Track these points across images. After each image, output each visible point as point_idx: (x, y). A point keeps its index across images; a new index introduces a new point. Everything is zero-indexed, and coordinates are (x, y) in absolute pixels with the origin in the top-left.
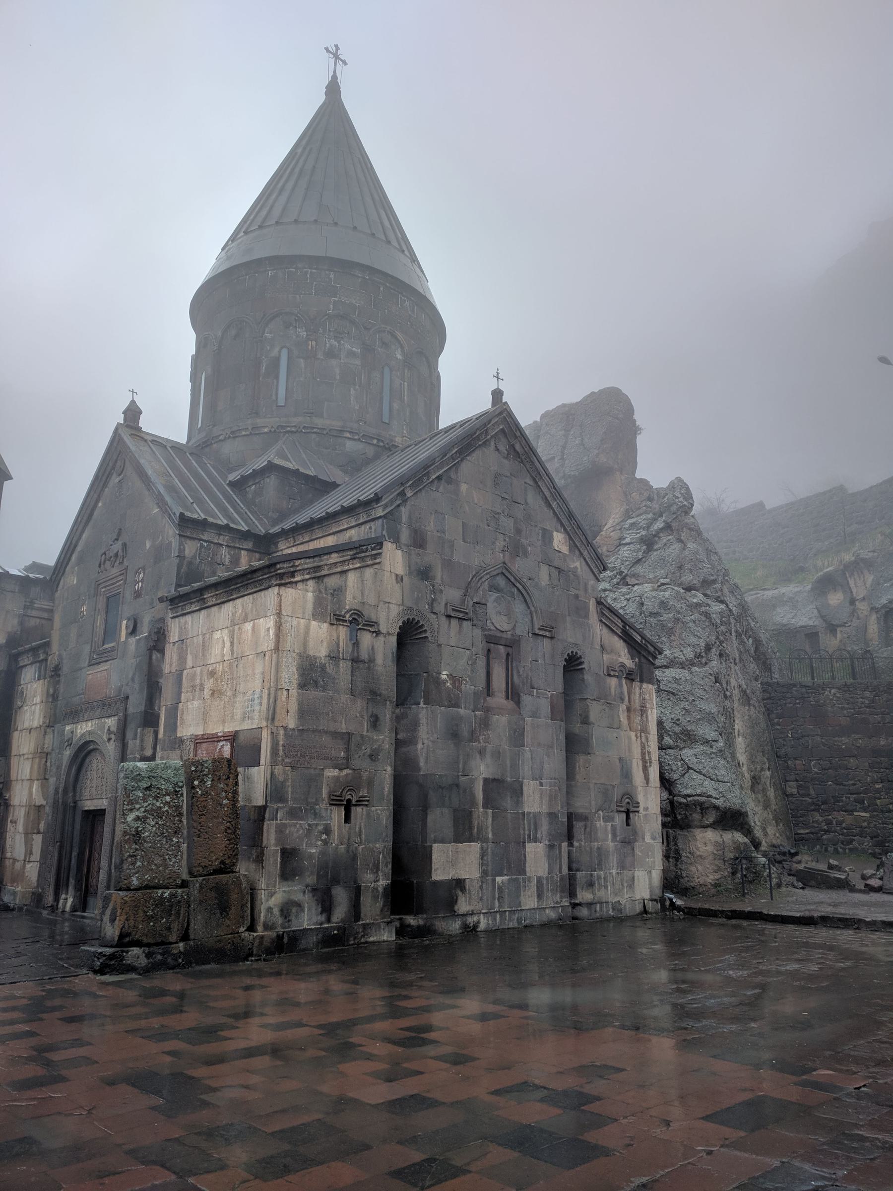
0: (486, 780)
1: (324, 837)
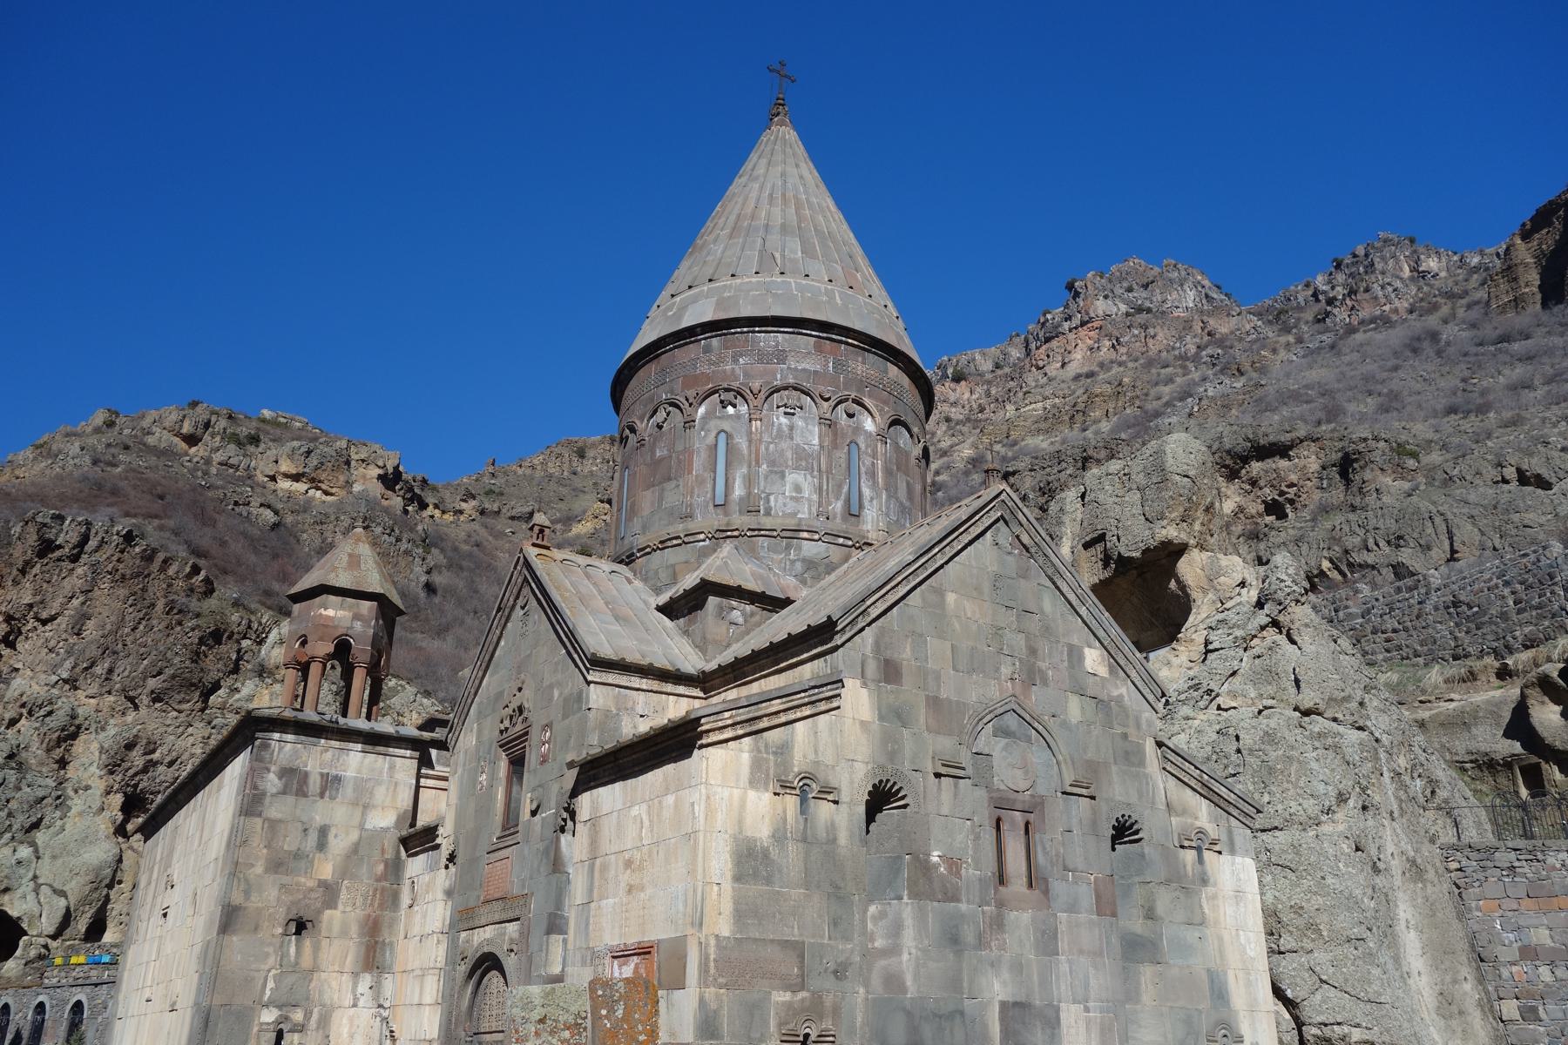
0: (1003, 1005)
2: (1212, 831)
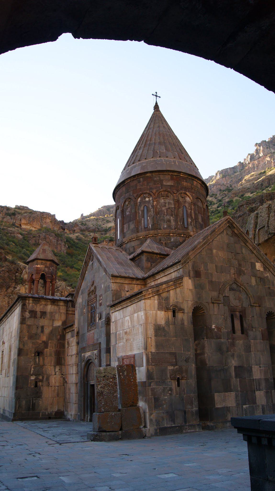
0: (235, 367)
1: (170, 392)
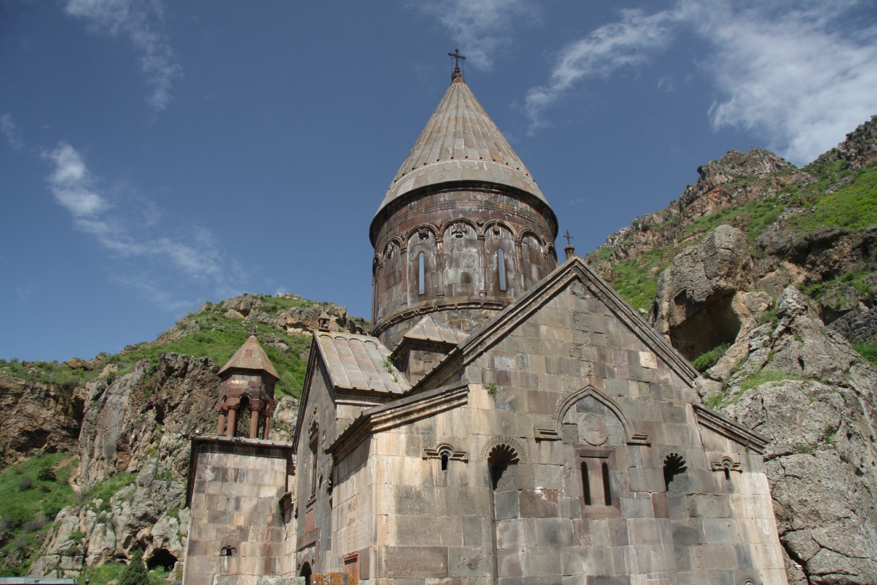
2: (735, 458)
